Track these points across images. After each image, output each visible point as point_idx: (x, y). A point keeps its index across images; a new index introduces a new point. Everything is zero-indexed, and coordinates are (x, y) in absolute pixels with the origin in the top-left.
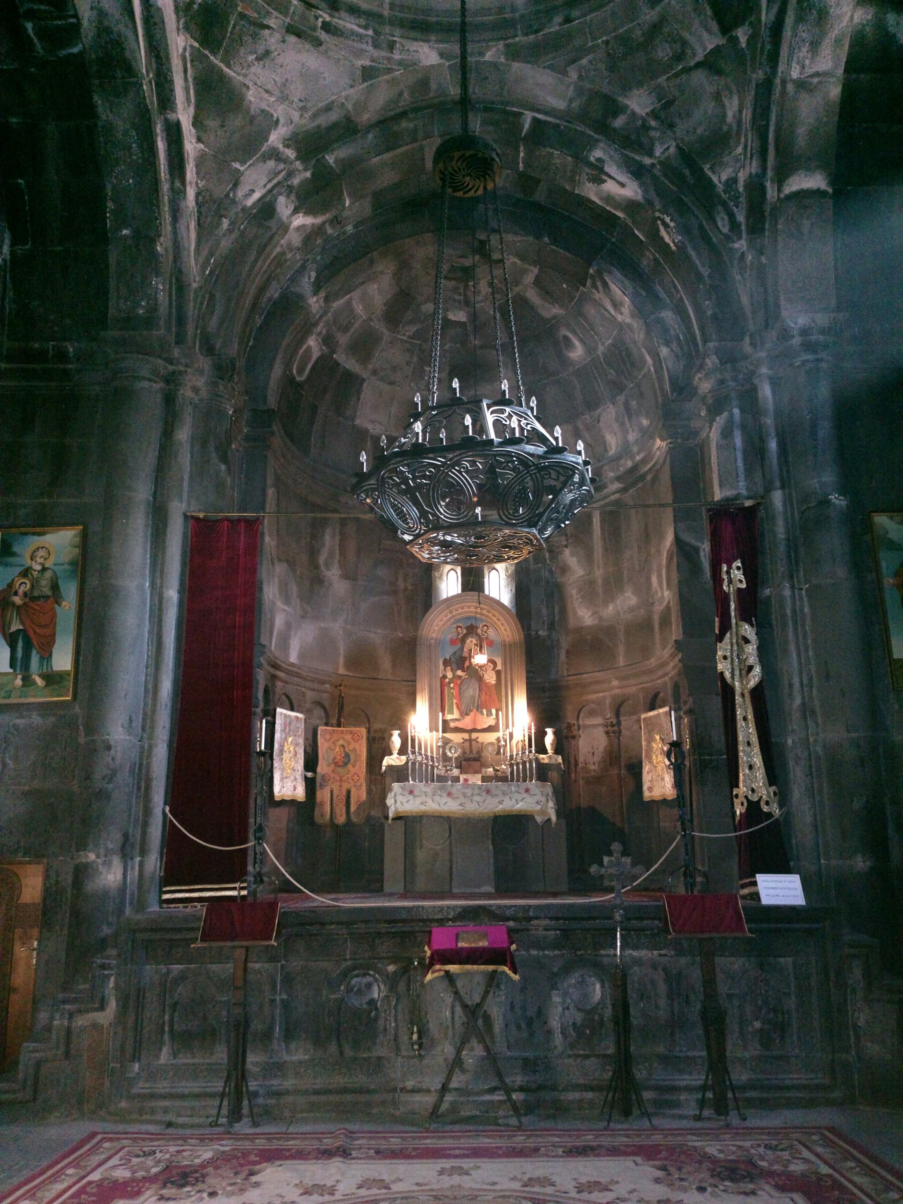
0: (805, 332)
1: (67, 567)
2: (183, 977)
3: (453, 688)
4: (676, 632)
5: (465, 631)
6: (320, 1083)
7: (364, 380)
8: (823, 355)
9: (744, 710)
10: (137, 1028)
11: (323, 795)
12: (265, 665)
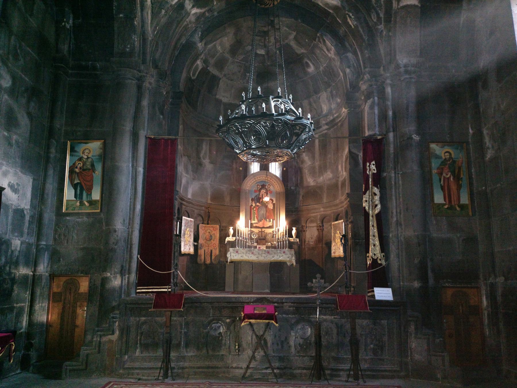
0: (405, 66)
1: (97, 157)
2: (145, 323)
4: (347, 190)
6: (200, 364)
7: (220, 79)
8: (413, 76)
9: (373, 222)
10: (127, 342)
11: (201, 252)
12: (178, 199)
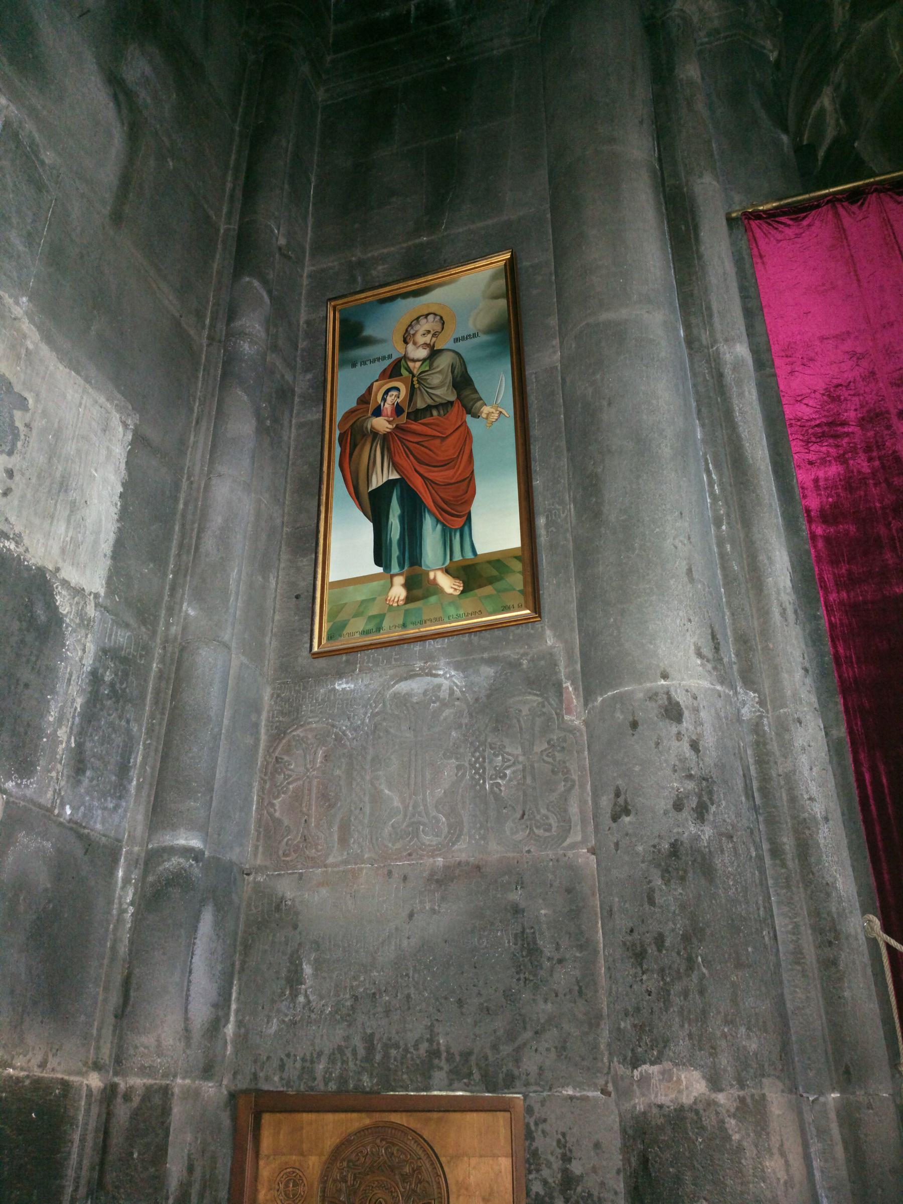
1: (484, 338)
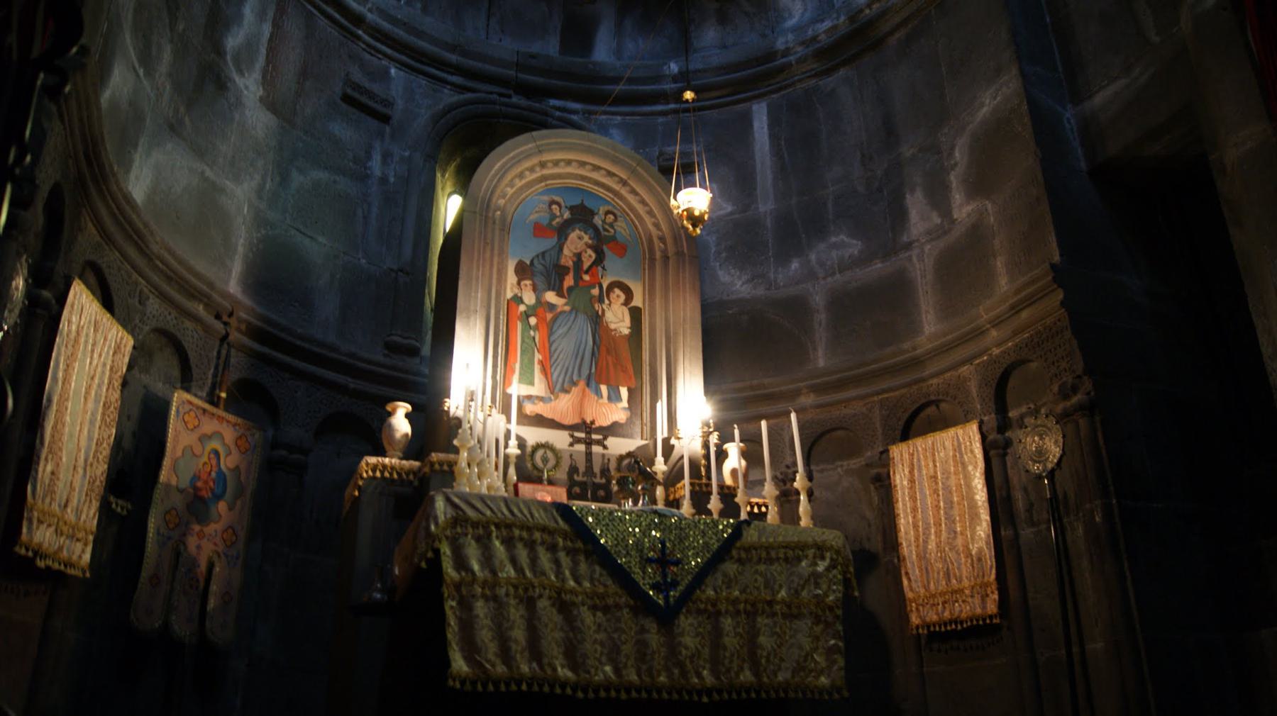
3: (536, 328)
5: (567, 215)
